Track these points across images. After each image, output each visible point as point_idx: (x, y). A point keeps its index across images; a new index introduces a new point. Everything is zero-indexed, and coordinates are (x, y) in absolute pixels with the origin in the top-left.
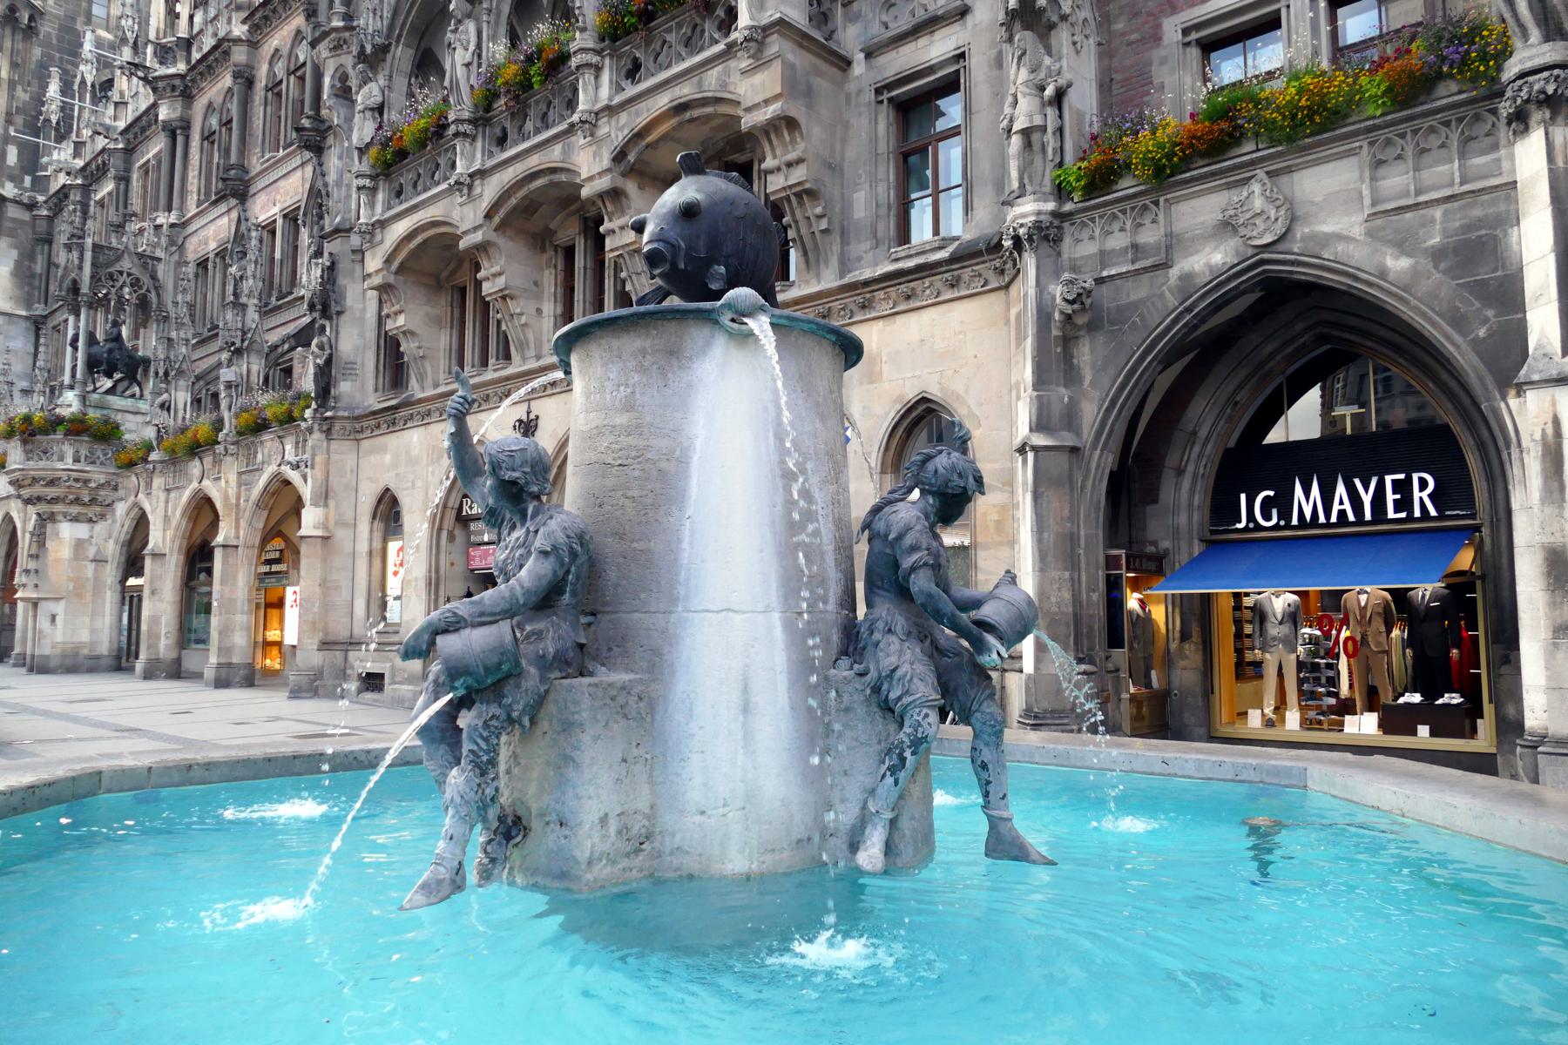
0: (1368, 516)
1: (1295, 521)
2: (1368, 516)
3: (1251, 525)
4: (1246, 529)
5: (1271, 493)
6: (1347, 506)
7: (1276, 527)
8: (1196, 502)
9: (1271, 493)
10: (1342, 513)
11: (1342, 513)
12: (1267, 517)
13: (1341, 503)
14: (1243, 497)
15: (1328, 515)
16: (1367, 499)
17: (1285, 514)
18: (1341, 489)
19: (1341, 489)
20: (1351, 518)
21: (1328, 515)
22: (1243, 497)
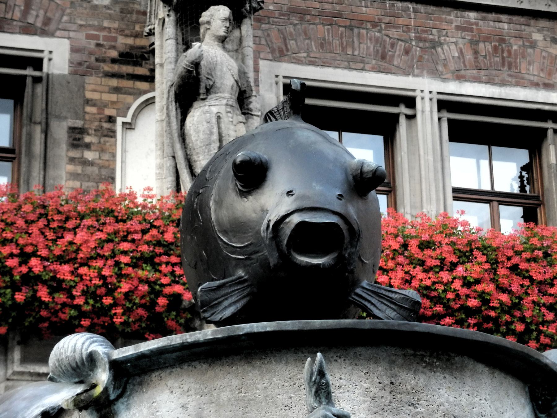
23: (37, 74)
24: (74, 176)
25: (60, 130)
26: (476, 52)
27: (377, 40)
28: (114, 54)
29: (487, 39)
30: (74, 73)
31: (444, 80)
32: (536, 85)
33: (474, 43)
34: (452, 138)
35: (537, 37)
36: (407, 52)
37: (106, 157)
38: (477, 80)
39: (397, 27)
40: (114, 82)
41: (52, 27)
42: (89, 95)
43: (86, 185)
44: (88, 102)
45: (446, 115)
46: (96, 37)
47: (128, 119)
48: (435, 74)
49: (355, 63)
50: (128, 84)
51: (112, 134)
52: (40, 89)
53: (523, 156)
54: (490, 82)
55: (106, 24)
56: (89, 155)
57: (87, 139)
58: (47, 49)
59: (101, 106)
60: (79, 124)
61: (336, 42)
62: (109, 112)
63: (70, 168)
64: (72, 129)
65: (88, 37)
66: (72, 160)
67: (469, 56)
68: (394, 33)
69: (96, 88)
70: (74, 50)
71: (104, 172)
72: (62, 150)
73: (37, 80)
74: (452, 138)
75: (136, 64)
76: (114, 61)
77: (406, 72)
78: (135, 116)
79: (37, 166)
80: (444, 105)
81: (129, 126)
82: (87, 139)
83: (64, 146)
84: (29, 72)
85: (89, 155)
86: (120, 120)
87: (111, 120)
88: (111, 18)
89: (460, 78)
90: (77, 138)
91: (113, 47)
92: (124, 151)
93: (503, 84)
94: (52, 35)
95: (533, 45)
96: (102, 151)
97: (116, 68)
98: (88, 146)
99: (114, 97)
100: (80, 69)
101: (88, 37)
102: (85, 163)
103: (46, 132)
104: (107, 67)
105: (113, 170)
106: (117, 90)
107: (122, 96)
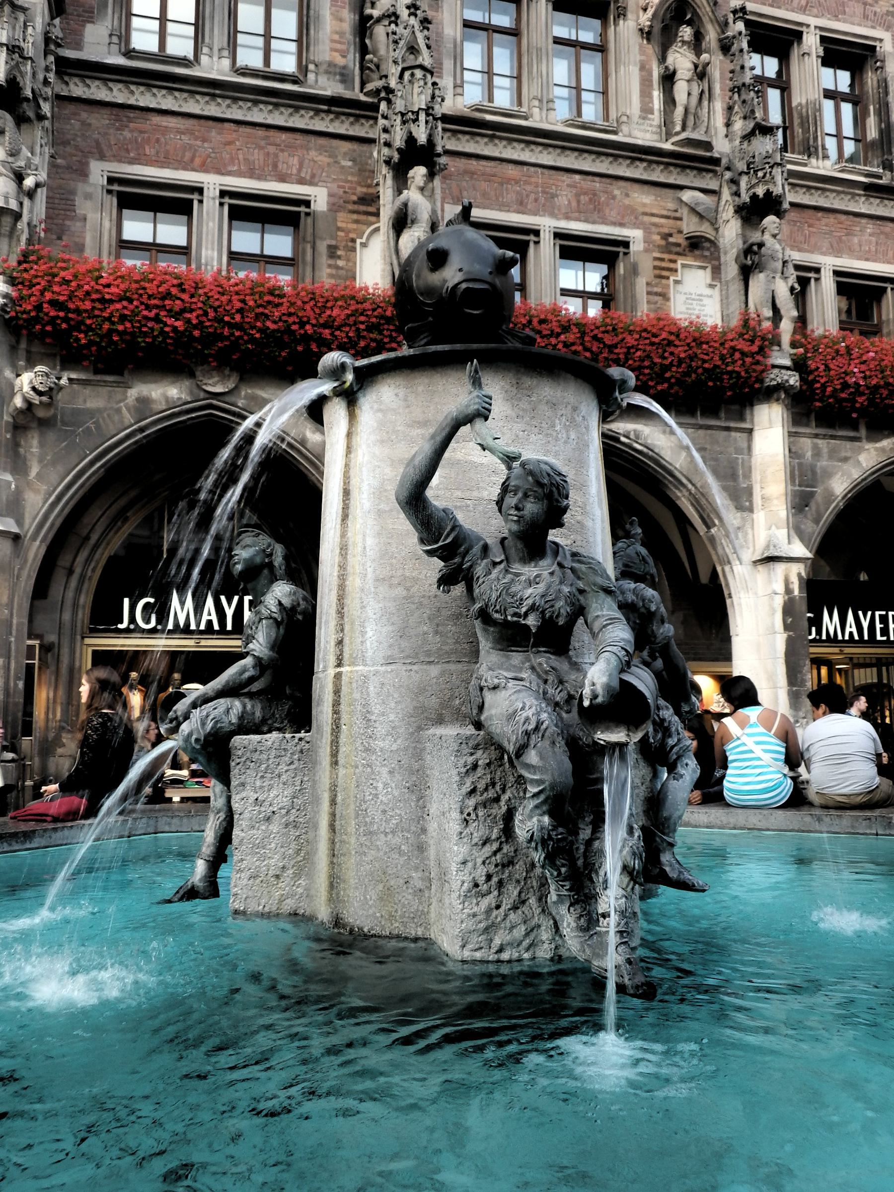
0: (229, 627)
1: (170, 626)
2: (229, 627)
3: (132, 627)
4: (127, 630)
5: (152, 600)
6: (214, 618)
7: (154, 631)
8: (82, 600)
9: (152, 600)
10: (210, 622)
11: (210, 622)
12: (148, 622)
13: (209, 614)
14: (126, 601)
15: (198, 625)
16: (229, 612)
17: (162, 617)
18: (210, 602)
19: (210, 602)
20: (216, 627)
21: (198, 625)
22: (126, 601)
23: (307, 210)
24: (331, 276)
25: (322, 247)
26: (578, 202)
27: (518, 193)
28: (355, 198)
29: (585, 194)
30: (330, 210)
31: (558, 219)
32: (614, 224)
33: (578, 195)
34: (562, 257)
35: (617, 192)
36: (536, 200)
37: (350, 264)
38: (578, 219)
39: (530, 184)
40: (355, 216)
41: (316, 180)
42: (340, 224)
43: (339, 281)
44: (339, 229)
45: (559, 242)
46: (343, 187)
47: (364, 240)
48: (553, 215)
49: (503, 207)
50: (363, 218)
51: (354, 249)
52: (309, 220)
53: (604, 269)
54: (586, 221)
55: (349, 178)
56: (340, 263)
57: (339, 253)
58: (313, 194)
59: (347, 232)
60: (333, 243)
61: (493, 193)
62: (352, 235)
63: (329, 271)
64: (330, 247)
65: (339, 187)
66: (330, 266)
67: (574, 204)
68: (529, 188)
69: (344, 220)
70: (330, 195)
71: (350, 274)
72: (323, 259)
73: (308, 214)
74: (562, 257)
75: (369, 205)
76: (354, 203)
77: (535, 214)
78: (368, 239)
79: (309, 270)
80: (558, 235)
81: (364, 245)
82: (339, 253)
83: (325, 257)
84: (303, 209)
85: (340, 263)
86: (358, 241)
87: (353, 241)
88: (352, 174)
89: (568, 218)
90: (332, 252)
91: (354, 194)
92: (361, 261)
93: (594, 223)
94: (316, 185)
95: (614, 198)
96: (348, 260)
97: (356, 207)
98: (339, 257)
99: (355, 226)
100: (334, 207)
101: (339, 187)
102: (338, 268)
103: (314, 248)
104: (350, 207)
105: (355, 273)
106: (357, 222)
107: (360, 226)
